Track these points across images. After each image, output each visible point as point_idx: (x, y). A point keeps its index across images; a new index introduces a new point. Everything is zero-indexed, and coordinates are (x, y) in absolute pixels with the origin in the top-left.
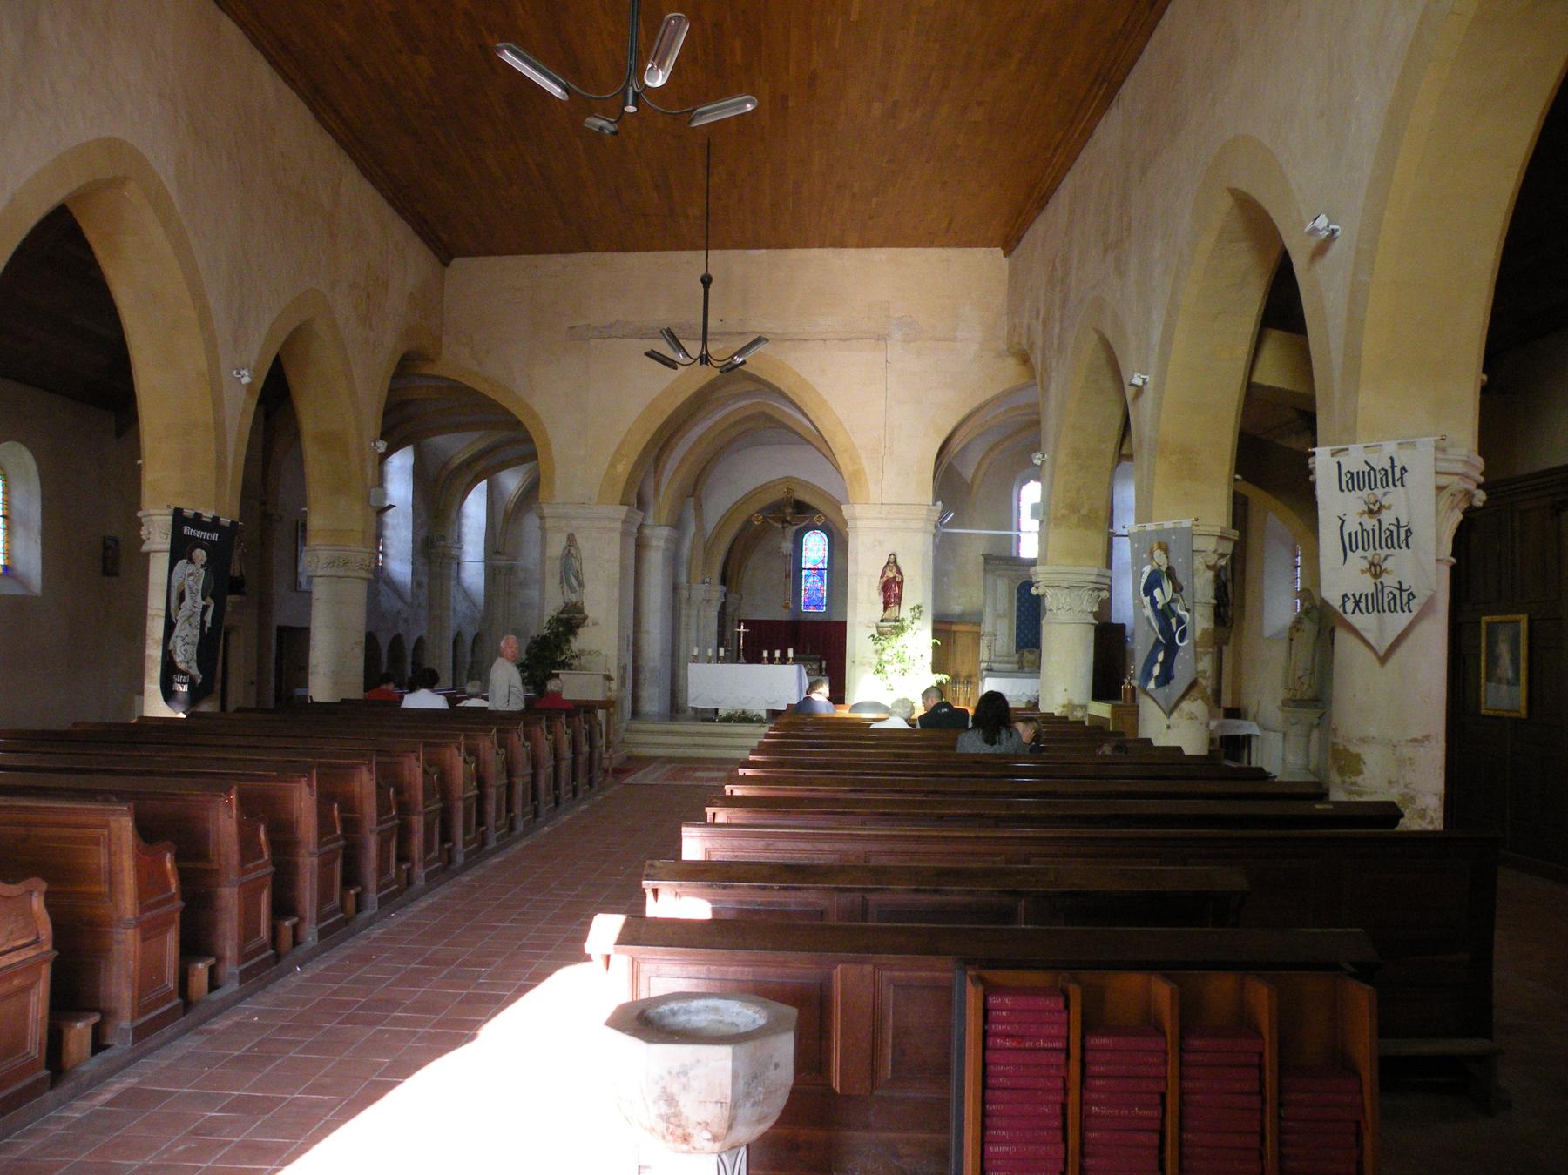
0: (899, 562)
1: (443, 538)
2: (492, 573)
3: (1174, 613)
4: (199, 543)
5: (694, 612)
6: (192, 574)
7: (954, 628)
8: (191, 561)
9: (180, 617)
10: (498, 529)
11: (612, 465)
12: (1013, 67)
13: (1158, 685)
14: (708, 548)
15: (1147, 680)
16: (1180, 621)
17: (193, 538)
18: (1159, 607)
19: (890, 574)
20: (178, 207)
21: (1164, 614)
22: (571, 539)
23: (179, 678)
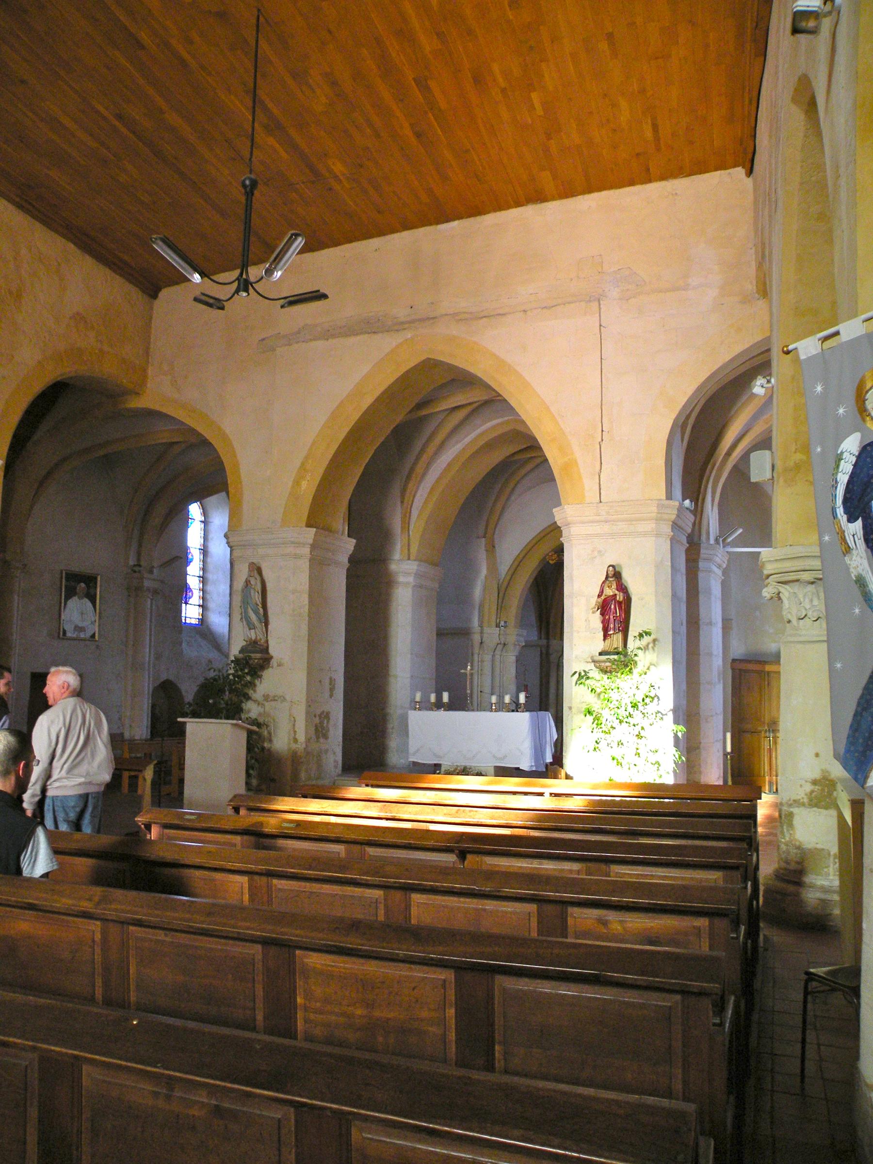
0: (627, 577)
5: (488, 658)
7: (768, 668)
11: (297, 483)
14: (503, 592)
19: (609, 592)
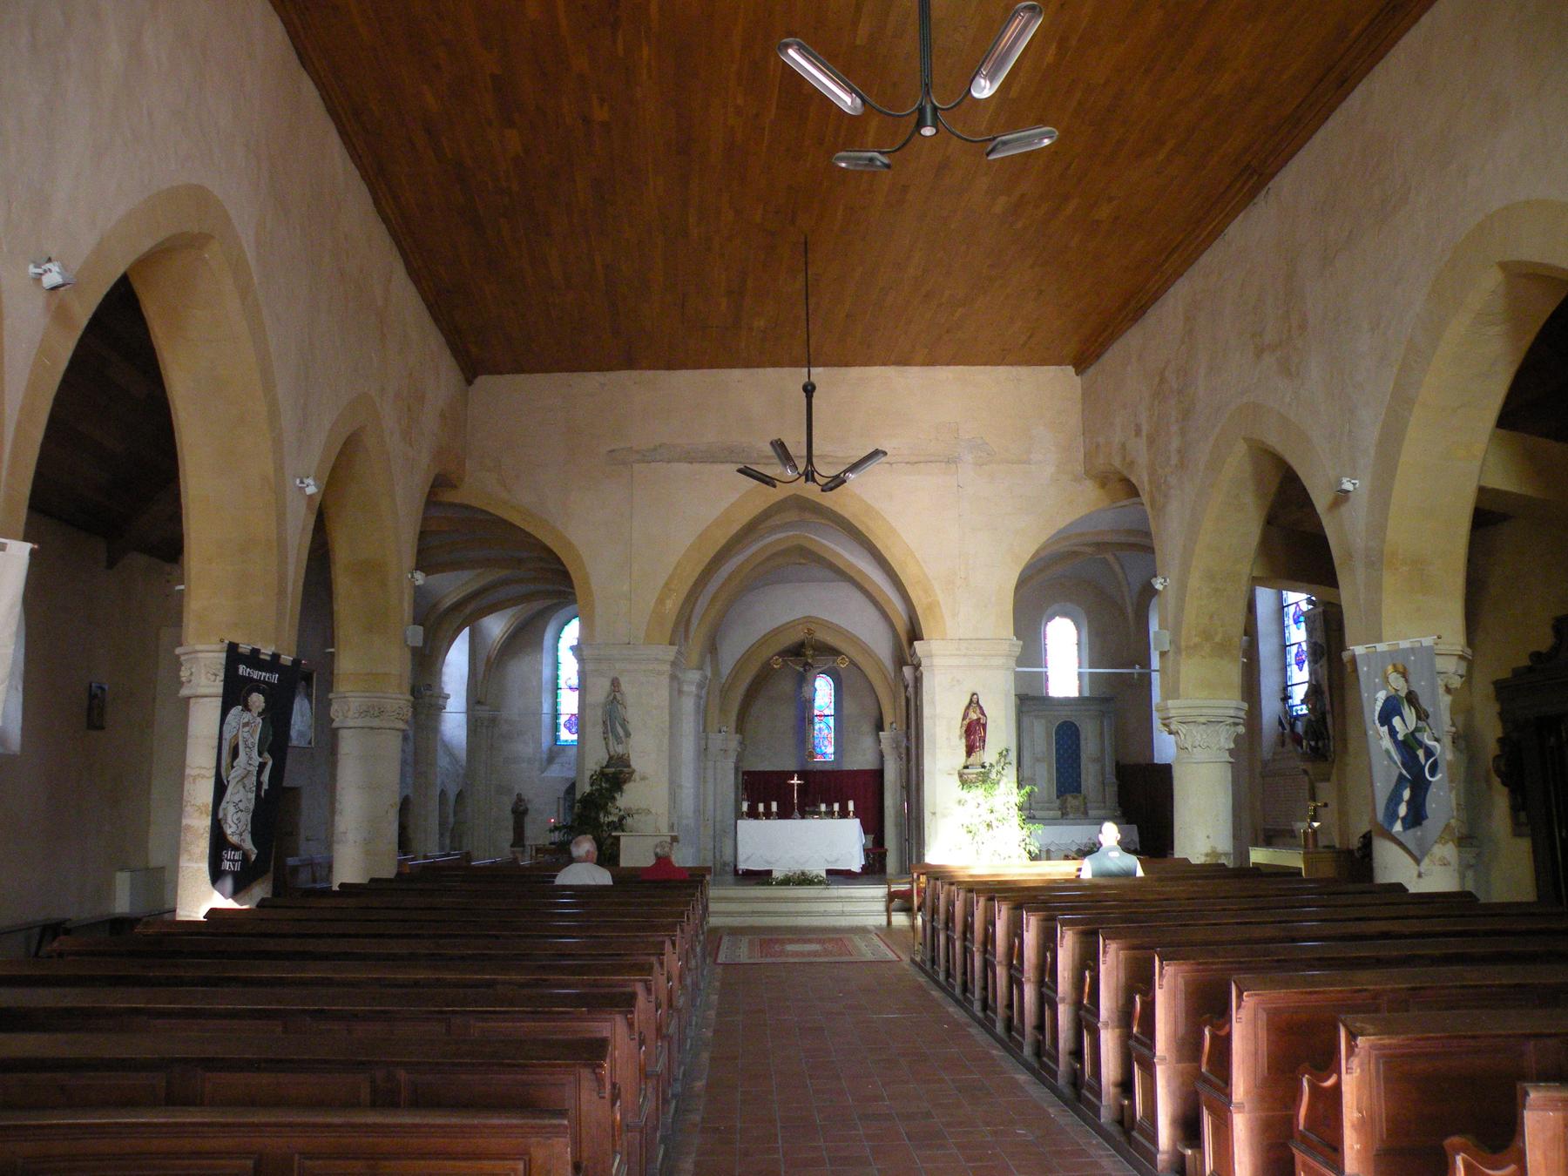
1: (429, 687)
2: (475, 725)
3: (1421, 744)
4: (256, 686)
6: (248, 724)
8: (247, 708)
9: (233, 777)
10: (480, 677)
11: (661, 601)
12: (1161, 157)
13: (1406, 827)
15: (1392, 823)
16: (1429, 753)
17: (250, 679)
18: (1400, 737)
19: (973, 716)
20: (256, 280)
21: (1408, 747)
22: (615, 683)
23: (230, 854)
